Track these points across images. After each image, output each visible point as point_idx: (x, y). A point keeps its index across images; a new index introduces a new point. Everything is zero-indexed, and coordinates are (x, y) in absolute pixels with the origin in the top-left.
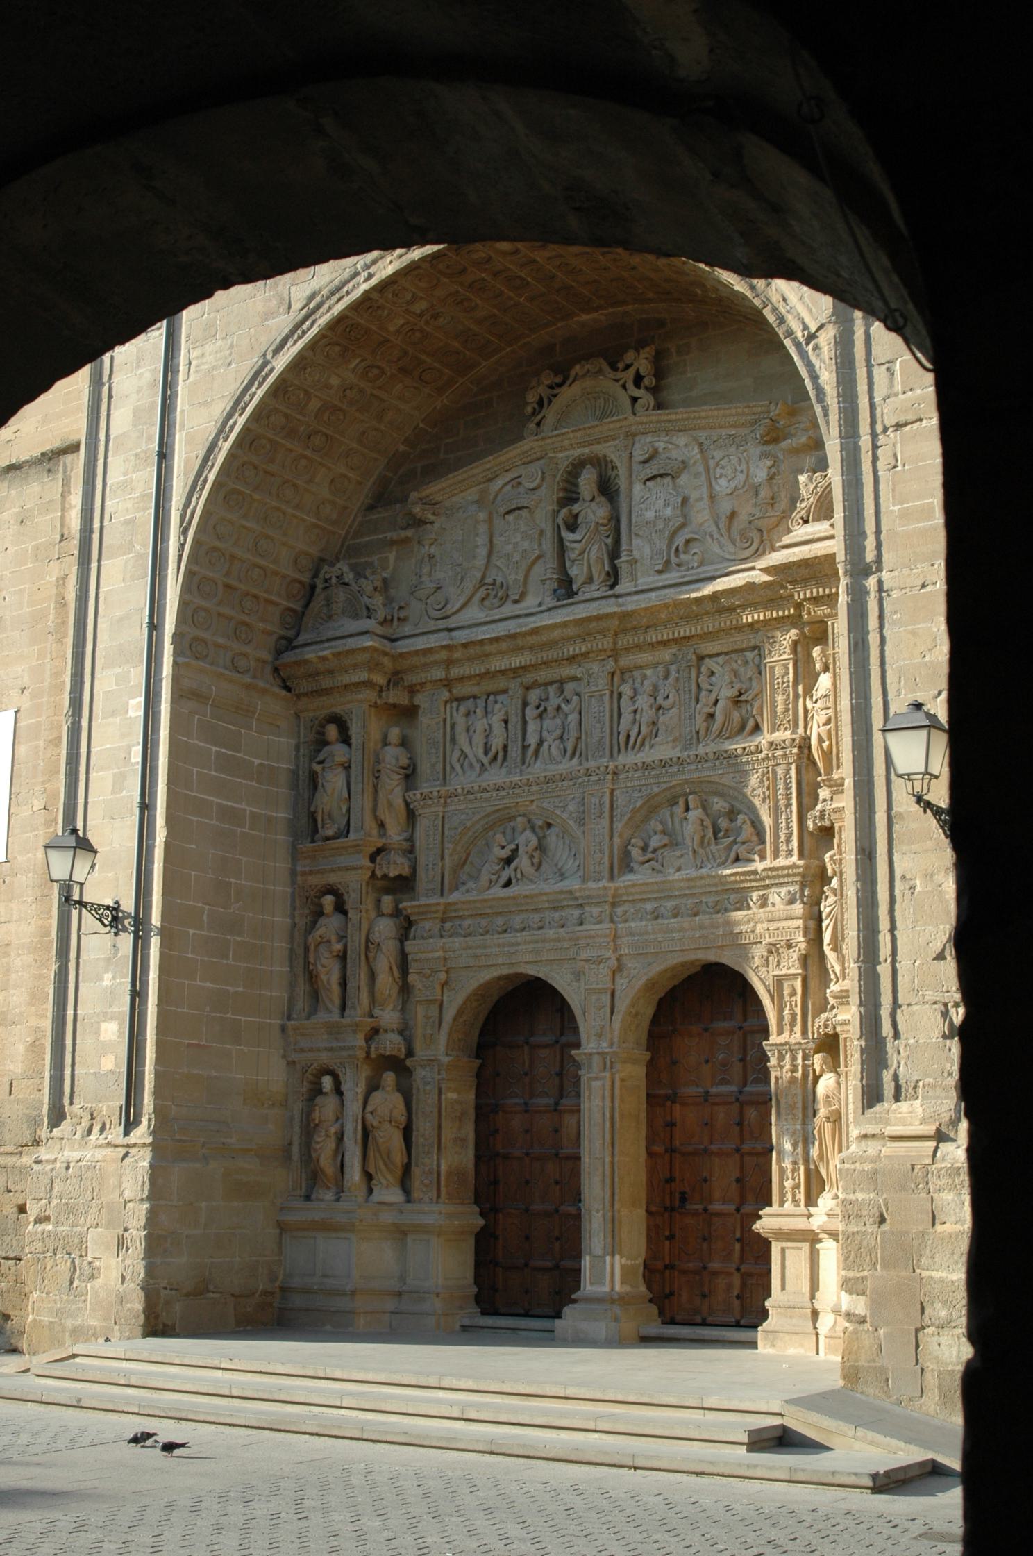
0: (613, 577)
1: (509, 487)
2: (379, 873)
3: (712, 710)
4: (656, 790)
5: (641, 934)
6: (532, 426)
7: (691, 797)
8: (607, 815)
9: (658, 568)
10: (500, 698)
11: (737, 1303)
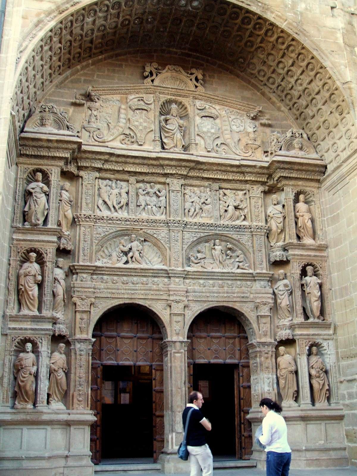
0: (185, 148)
1: (136, 100)
4: (202, 235)
5: (200, 292)
7: (217, 241)
8: (180, 241)
9: (209, 150)
10: (122, 183)
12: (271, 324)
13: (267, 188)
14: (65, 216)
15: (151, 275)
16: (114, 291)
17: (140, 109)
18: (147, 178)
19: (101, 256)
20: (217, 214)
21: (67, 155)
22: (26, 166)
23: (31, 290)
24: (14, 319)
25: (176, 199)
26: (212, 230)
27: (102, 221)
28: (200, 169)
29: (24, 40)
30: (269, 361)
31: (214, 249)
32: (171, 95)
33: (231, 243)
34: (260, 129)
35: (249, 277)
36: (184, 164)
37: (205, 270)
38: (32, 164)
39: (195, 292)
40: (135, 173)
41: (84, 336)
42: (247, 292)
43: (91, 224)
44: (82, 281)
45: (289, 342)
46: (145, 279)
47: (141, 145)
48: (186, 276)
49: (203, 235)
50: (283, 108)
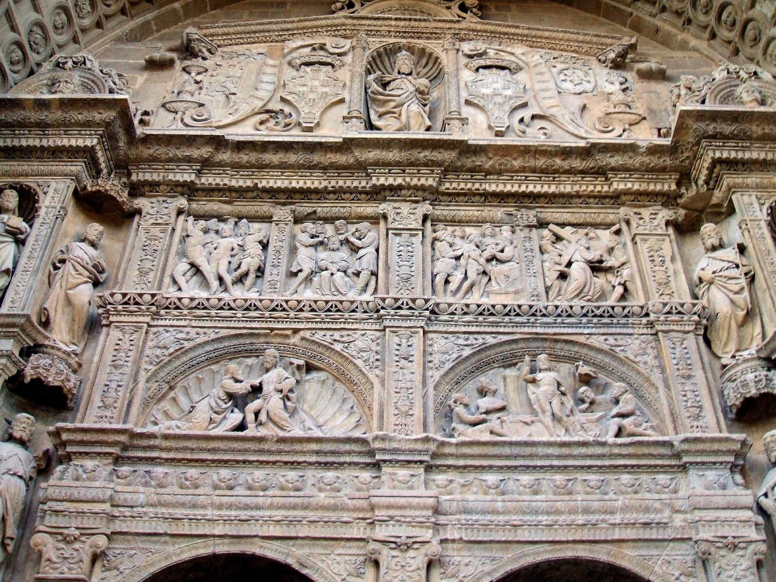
4: (490, 340)
5: (484, 512)
8: (417, 357)
13: (682, 212)
14: (69, 302)
15: (314, 459)
16: (178, 512)
18: (323, 208)
19: (166, 413)
27: (175, 312)
28: (473, 170)
33: (586, 363)
34: (638, 86)
35: (662, 457)
36: (424, 155)
39: (466, 511)
40: (290, 195)
42: (657, 505)
43: (141, 319)
46: (293, 474)
47: (310, 130)
49: (494, 341)
50: (693, 42)
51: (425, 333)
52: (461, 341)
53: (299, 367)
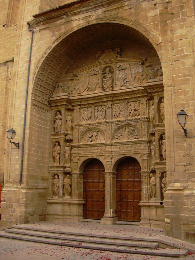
0: (112, 87)
1: (93, 71)
2: (67, 139)
3: (131, 112)
4: (120, 125)
5: (117, 151)
6: (98, 60)
7: (126, 127)
8: (110, 130)
9: (121, 86)
10: (90, 108)
11: (133, 217)
12: (148, 163)
15: (98, 146)
16: (85, 154)
17: (94, 75)
18: (98, 104)
19: (83, 140)
20: (126, 115)
21: (65, 103)
22: (54, 110)
23: (56, 157)
24: (52, 167)
25: (109, 111)
26: (124, 123)
29: (35, 69)
30: (146, 180)
31: (125, 131)
32: (107, 64)
34: (145, 69)
37: (120, 141)
38: (55, 109)
39: (115, 151)
41: (76, 172)
42: (137, 149)
44: (75, 151)
45: (153, 172)
48: (112, 145)
51: (111, 125)
52: (116, 126)
53: (97, 132)
